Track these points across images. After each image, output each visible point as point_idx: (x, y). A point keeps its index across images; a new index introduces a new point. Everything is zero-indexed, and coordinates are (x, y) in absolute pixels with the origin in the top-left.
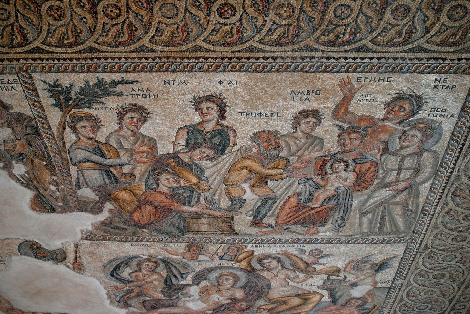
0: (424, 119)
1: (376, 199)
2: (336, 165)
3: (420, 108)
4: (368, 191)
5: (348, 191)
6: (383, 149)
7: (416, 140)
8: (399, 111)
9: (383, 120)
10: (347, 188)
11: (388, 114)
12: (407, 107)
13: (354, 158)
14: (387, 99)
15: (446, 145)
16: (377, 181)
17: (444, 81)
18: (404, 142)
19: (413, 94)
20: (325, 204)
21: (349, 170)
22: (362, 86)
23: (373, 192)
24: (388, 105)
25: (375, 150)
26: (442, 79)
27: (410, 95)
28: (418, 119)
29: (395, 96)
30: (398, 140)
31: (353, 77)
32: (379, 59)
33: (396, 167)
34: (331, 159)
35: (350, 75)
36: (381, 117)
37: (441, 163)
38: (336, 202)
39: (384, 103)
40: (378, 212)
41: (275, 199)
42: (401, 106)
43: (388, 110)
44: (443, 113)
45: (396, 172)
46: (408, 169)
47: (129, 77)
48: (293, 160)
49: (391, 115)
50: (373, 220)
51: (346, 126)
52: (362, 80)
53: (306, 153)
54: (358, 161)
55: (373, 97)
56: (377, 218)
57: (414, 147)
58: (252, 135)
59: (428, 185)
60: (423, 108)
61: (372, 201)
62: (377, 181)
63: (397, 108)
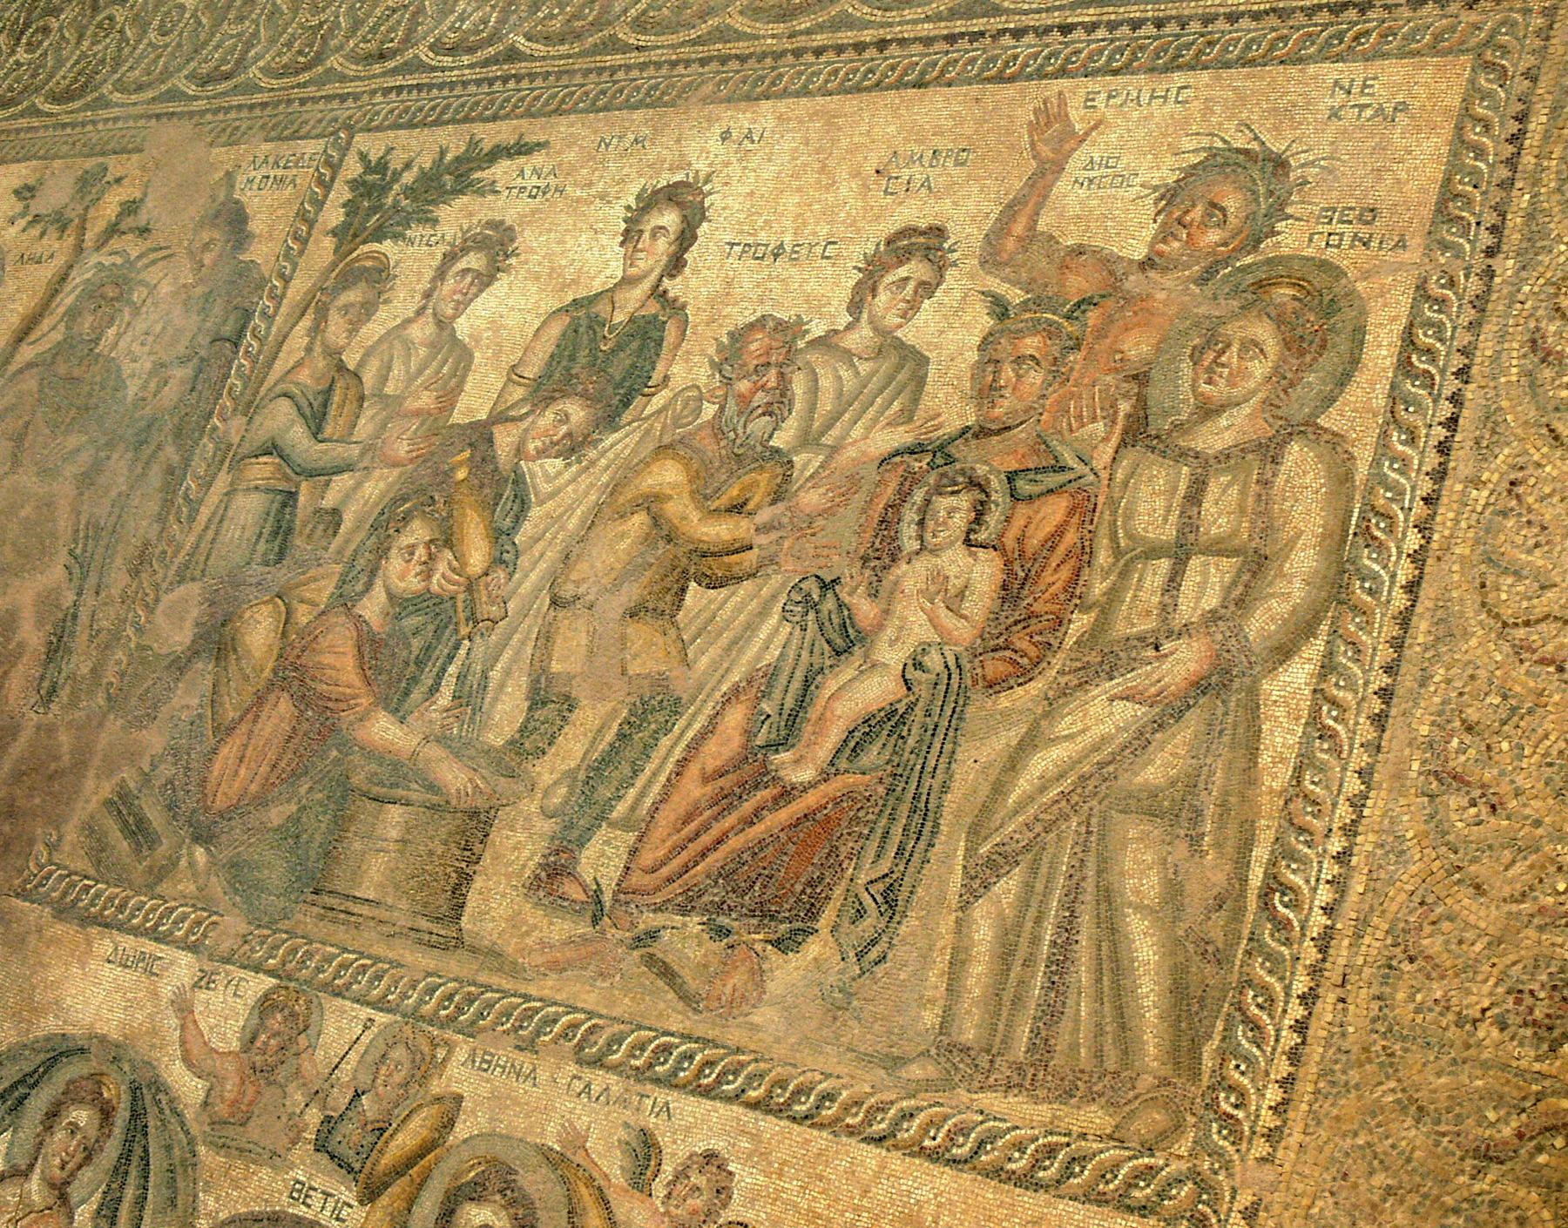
0: (1291, 258)
1: (1059, 753)
2: (943, 503)
3: (1279, 210)
4: (1036, 687)
5: (955, 677)
6: (1128, 416)
7: (1259, 369)
8: (1203, 225)
9: (1147, 264)
10: (952, 664)
11: (1164, 241)
12: (1232, 203)
13: (1015, 466)
14: (1167, 174)
15: (1380, 401)
16: (1080, 623)
17: (1365, 86)
18: (1209, 382)
19: (1255, 146)
20: (843, 764)
21: (982, 536)
22: (1095, 127)
23: (1054, 702)
24: (1169, 196)
25: (1094, 419)
26: (1358, 82)
27: (1246, 152)
28: (1269, 261)
29: (1195, 159)
30: (1186, 367)
31: (1074, 91)
32: (1159, 24)
33: (1169, 533)
34: (932, 466)
35: (1064, 83)
36: (1140, 253)
37: (1362, 518)
38: (887, 754)
39: (1156, 188)
40: (1053, 866)
41: (676, 706)
42: (1214, 205)
43: (1164, 224)
44: (1364, 231)
45: (1164, 565)
46: (1219, 549)
47: (534, 131)
48: (805, 466)
49: (1176, 245)
50: (1020, 925)
51: (1016, 296)
52: (1100, 101)
53: (857, 432)
54: (1024, 486)
55: (1125, 157)
56: (1038, 921)
57: (1246, 410)
58: (725, 340)
59: (1298, 674)
60: (1289, 210)
61: (1041, 763)
62: (1080, 623)
63: (1197, 213)
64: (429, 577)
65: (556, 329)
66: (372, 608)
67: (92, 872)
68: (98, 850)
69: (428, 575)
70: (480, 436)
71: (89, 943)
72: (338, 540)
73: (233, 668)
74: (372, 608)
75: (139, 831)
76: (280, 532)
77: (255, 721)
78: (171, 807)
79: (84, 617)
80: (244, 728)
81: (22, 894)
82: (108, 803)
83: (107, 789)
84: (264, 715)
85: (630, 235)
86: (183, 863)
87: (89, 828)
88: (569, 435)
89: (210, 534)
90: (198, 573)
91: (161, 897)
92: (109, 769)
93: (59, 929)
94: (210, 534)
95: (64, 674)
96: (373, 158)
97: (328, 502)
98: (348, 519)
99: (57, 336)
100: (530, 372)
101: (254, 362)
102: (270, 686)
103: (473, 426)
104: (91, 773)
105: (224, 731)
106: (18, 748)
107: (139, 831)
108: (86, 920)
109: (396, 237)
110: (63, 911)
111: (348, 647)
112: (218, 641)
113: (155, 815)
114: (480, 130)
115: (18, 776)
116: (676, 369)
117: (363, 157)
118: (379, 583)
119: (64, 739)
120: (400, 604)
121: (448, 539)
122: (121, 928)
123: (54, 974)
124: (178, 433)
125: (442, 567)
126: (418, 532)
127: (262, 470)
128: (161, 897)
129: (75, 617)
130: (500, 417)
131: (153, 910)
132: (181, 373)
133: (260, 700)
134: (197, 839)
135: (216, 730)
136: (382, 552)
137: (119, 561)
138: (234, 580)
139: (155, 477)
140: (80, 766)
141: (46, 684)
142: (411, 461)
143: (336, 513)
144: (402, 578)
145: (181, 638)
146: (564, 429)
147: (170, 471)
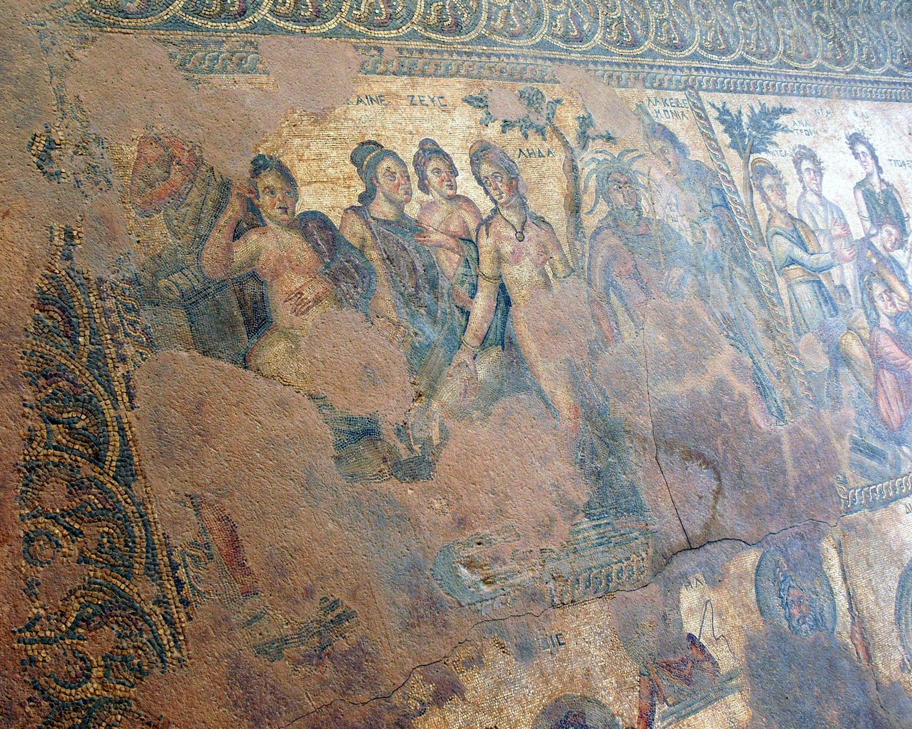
64: (895, 306)
65: (860, 194)
66: (885, 323)
67: (870, 482)
68: (864, 471)
69: (894, 304)
70: (866, 242)
71: (895, 511)
72: (852, 299)
73: (857, 367)
74: (885, 323)
75: (873, 453)
76: (826, 298)
77: (882, 386)
78: (879, 437)
79: (764, 368)
80: (881, 389)
81: (849, 511)
82: (852, 449)
83: (847, 444)
84: (883, 380)
85: (856, 155)
86: (902, 457)
87: (852, 465)
88: (896, 239)
89: (796, 309)
90: (805, 328)
91: (905, 475)
92: (841, 436)
93: (878, 515)
94: (796, 309)
95: (779, 401)
96: (720, 106)
97: (837, 283)
98: (849, 287)
99: (603, 207)
100: (866, 214)
101: (746, 217)
102: (877, 370)
103: (863, 239)
104: (834, 441)
105: (874, 395)
106: (786, 448)
107: (873, 453)
108: (886, 503)
109: (766, 151)
110: (872, 507)
111: (890, 342)
112: (840, 358)
113: (875, 443)
114: (764, 99)
115: (797, 460)
116: (908, 210)
117: (713, 106)
118: (880, 312)
119: (809, 432)
120: (895, 319)
121: (890, 290)
122: (895, 499)
123: (892, 534)
124: (735, 259)
125: (896, 301)
126: (878, 289)
127: (795, 272)
128: (905, 475)
129: (760, 369)
130: (869, 236)
131: (907, 481)
132: (709, 225)
133: (877, 377)
134: (899, 444)
135: (871, 396)
136: (872, 300)
137: (759, 334)
138: (823, 327)
139: (743, 287)
140: (826, 440)
141: (774, 409)
142: (853, 257)
143: (843, 286)
144: (887, 308)
145: (823, 363)
146: (893, 238)
147: (747, 281)
